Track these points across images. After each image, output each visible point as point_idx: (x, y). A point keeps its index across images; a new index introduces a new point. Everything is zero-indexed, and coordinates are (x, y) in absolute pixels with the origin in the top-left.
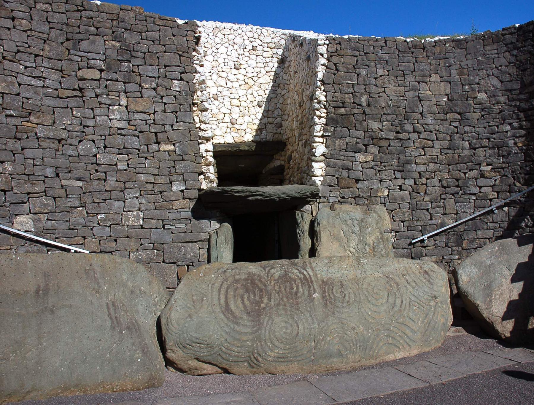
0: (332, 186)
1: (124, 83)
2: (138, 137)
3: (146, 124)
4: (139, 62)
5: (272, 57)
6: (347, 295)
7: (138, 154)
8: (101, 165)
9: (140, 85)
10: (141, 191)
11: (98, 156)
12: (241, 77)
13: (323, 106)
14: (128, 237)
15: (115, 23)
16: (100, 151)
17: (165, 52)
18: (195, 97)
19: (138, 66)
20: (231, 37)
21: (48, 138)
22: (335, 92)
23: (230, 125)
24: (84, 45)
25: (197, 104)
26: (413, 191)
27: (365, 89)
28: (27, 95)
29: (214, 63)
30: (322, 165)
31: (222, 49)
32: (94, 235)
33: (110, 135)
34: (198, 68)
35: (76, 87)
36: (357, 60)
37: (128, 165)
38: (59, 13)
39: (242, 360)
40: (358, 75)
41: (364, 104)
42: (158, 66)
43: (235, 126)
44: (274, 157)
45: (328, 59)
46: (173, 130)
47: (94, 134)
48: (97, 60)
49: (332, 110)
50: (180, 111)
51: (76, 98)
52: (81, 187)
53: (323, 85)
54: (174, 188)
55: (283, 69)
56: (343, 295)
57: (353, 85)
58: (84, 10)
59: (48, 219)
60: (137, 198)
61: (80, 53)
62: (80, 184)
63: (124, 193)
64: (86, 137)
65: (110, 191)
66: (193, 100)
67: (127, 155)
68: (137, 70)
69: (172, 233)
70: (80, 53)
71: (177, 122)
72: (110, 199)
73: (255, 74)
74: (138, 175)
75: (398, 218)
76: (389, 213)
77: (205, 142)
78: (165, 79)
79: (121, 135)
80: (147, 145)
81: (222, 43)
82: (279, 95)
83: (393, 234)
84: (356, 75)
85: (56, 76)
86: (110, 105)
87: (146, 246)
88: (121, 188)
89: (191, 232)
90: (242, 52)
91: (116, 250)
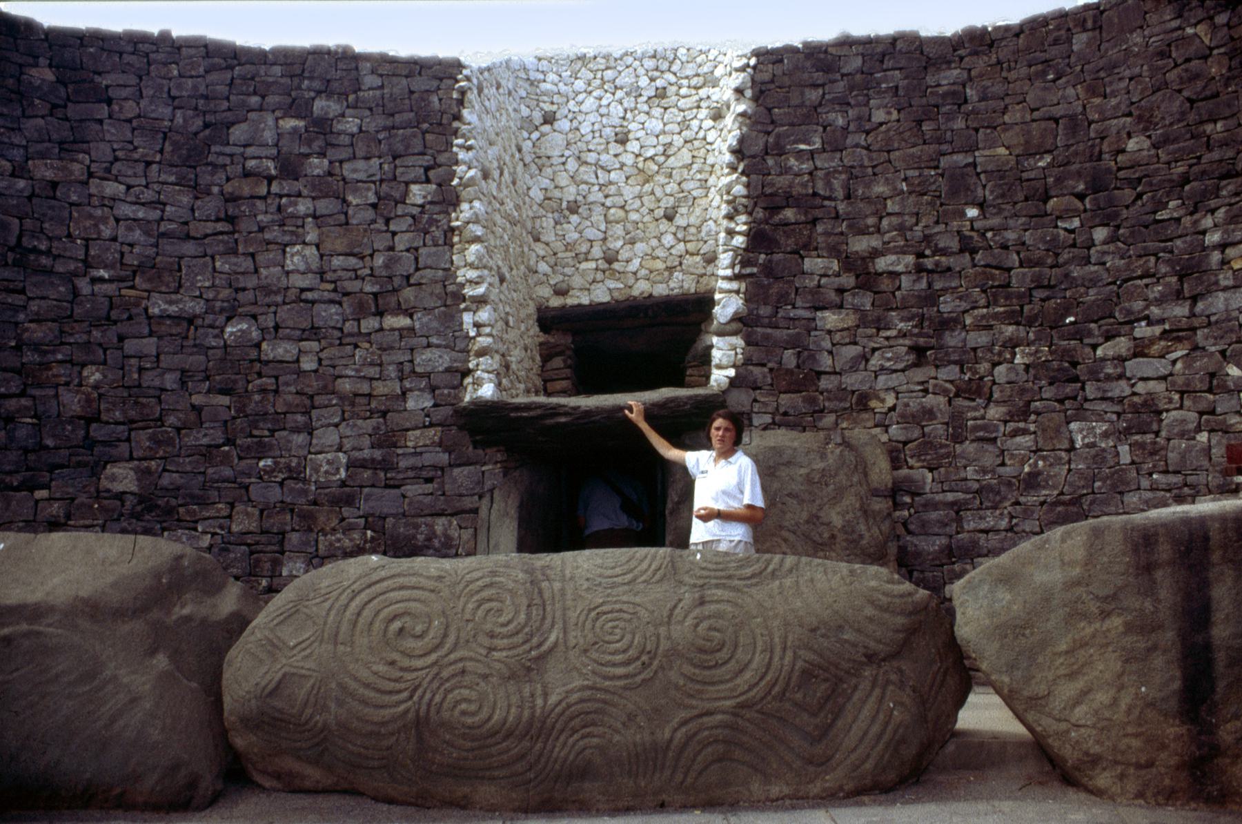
0: (760, 388)
1: (314, 198)
2: (340, 303)
3: (357, 277)
4: (344, 155)
5: (699, 107)
6: (628, 637)
7: (340, 339)
8: (268, 362)
9: (344, 201)
10: (343, 412)
11: (264, 346)
12: (628, 159)
13: (741, 208)
14: (315, 503)
15: (296, 80)
16: (267, 336)
17: (393, 128)
18: (453, 215)
19: (341, 162)
20: (609, 74)
21: (169, 317)
22: (769, 174)
23: (602, 264)
24: (238, 133)
25: (458, 227)
26: (957, 395)
27: (841, 159)
28: (130, 239)
29: (570, 136)
30: (738, 341)
31: (590, 103)
32: (250, 500)
33: (284, 303)
34: (462, 155)
35: (222, 215)
36: (824, 94)
37: (320, 360)
38: (192, 77)
39: (376, 763)
40: (825, 128)
41: (840, 193)
42: (380, 157)
43: (616, 266)
44: (703, 327)
45: (755, 99)
46: (410, 285)
47: (256, 303)
48: (260, 158)
49: (760, 214)
50: (425, 245)
51: (221, 237)
52: (229, 408)
53: (740, 160)
54: (411, 404)
55: (721, 130)
56: (617, 637)
57: (812, 153)
58: (239, 65)
59: (165, 470)
60: (336, 425)
61: (228, 150)
62: (225, 400)
63: (310, 418)
64: (240, 310)
65: (285, 414)
66: (450, 221)
67: (319, 341)
68: (337, 171)
69: (404, 496)
70: (228, 150)
71: (417, 269)
72: (284, 429)
73: (660, 149)
74: (339, 380)
75: (919, 461)
76: (890, 452)
77: (474, 307)
78: (394, 183)
79: (306, 301)
80: (359, 320)
81: (590, 88)
82: (713, 189)
83: (907, 499)
84: (821, 129)
85: (185, 199)
86: (286, 245)
87: (350, 524)
88: (305, 406)
89: (444, 494)
90: (633, 105)
91: (293, 530)
